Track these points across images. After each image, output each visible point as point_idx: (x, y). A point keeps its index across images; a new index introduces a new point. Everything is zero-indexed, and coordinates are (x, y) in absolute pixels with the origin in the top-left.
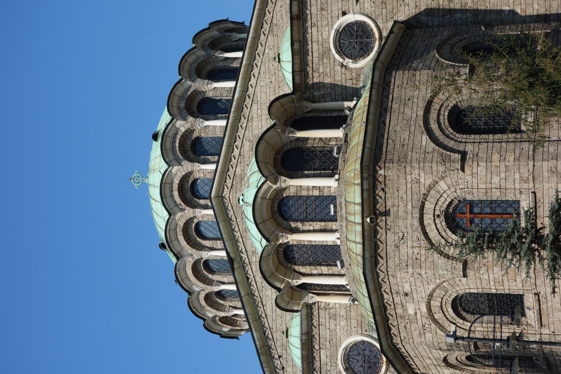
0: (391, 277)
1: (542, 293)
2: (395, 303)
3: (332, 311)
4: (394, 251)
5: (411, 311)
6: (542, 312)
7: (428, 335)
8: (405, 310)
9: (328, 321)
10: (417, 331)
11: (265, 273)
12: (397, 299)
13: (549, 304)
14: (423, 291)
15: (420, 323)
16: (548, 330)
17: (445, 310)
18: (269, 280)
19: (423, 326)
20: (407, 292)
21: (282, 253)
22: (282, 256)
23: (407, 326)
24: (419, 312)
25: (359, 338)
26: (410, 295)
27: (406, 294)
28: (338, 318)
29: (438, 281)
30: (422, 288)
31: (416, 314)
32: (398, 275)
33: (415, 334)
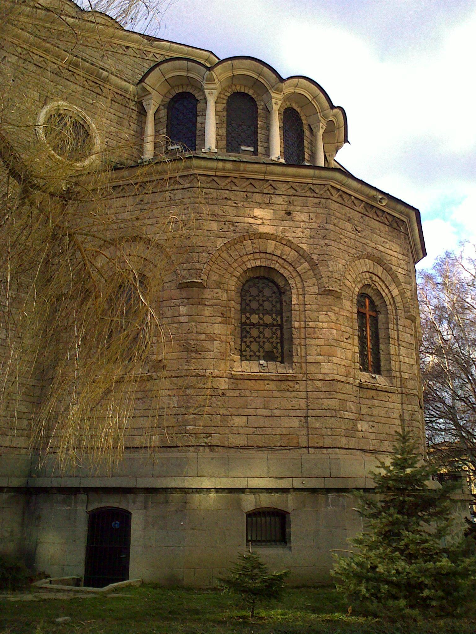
0: (317, 200)
1: (297, 386)
2: (272, 196)
3: (126, 123)
4: (345, 214)
5: (257, 212)
6: (261, 382)
7: (214, 226)
8: (260, 205)
9: (117, 113)
10: (221, 213)
11: (240, 61)
12: (279, 200)
13: (276, 394)
14: (295, 235)
15: (235, 219)
16: (227, 387)
17: (257, 256)
18: (230, 62)
19: (232, 223)
20: (294, 214)
21: (246, 92)
22: (243, 91)
23: (229, 202)
24: (259, 222)
25: (98, 142)
26: (288, 217)
27: (289, 214)
28: (119, 127)
29: (315, 257)
30: (301, 235)
31: (255, 217)
32: (321, 211)
33: (217, 210)
